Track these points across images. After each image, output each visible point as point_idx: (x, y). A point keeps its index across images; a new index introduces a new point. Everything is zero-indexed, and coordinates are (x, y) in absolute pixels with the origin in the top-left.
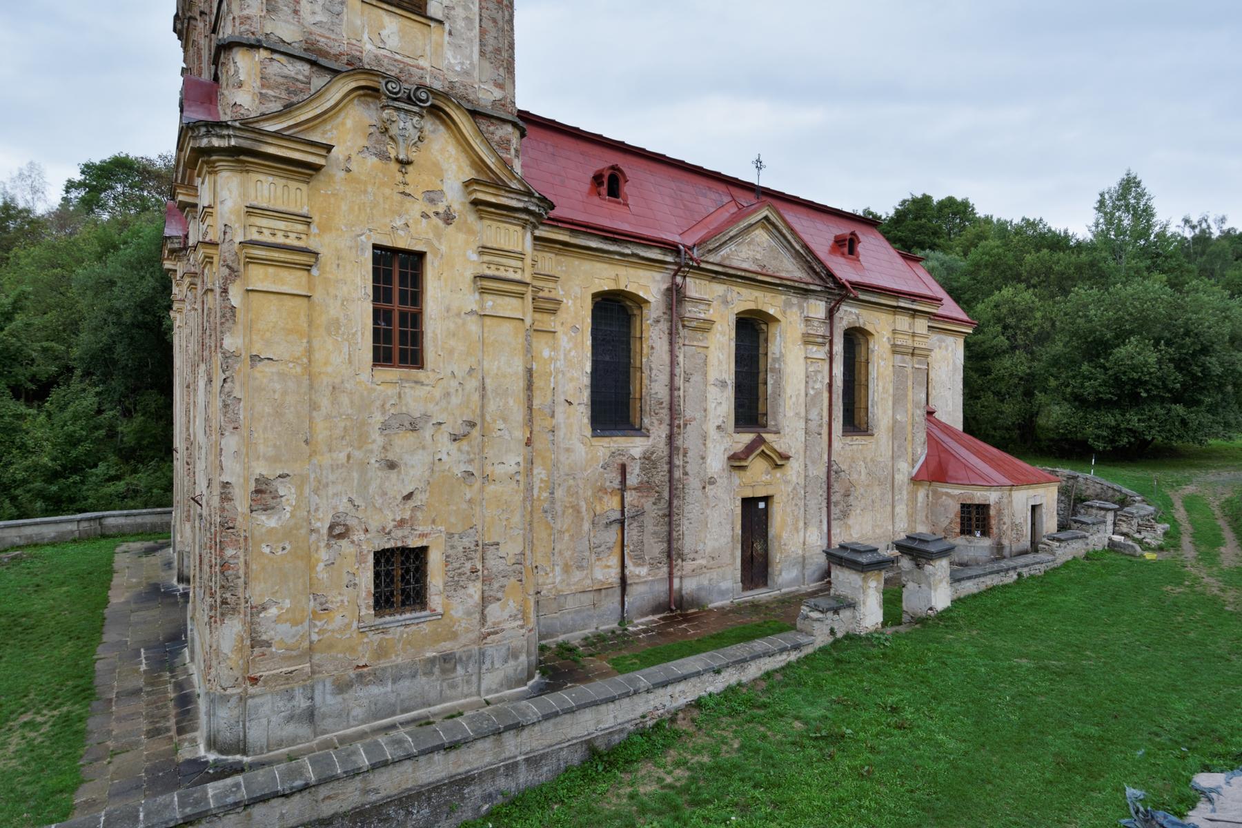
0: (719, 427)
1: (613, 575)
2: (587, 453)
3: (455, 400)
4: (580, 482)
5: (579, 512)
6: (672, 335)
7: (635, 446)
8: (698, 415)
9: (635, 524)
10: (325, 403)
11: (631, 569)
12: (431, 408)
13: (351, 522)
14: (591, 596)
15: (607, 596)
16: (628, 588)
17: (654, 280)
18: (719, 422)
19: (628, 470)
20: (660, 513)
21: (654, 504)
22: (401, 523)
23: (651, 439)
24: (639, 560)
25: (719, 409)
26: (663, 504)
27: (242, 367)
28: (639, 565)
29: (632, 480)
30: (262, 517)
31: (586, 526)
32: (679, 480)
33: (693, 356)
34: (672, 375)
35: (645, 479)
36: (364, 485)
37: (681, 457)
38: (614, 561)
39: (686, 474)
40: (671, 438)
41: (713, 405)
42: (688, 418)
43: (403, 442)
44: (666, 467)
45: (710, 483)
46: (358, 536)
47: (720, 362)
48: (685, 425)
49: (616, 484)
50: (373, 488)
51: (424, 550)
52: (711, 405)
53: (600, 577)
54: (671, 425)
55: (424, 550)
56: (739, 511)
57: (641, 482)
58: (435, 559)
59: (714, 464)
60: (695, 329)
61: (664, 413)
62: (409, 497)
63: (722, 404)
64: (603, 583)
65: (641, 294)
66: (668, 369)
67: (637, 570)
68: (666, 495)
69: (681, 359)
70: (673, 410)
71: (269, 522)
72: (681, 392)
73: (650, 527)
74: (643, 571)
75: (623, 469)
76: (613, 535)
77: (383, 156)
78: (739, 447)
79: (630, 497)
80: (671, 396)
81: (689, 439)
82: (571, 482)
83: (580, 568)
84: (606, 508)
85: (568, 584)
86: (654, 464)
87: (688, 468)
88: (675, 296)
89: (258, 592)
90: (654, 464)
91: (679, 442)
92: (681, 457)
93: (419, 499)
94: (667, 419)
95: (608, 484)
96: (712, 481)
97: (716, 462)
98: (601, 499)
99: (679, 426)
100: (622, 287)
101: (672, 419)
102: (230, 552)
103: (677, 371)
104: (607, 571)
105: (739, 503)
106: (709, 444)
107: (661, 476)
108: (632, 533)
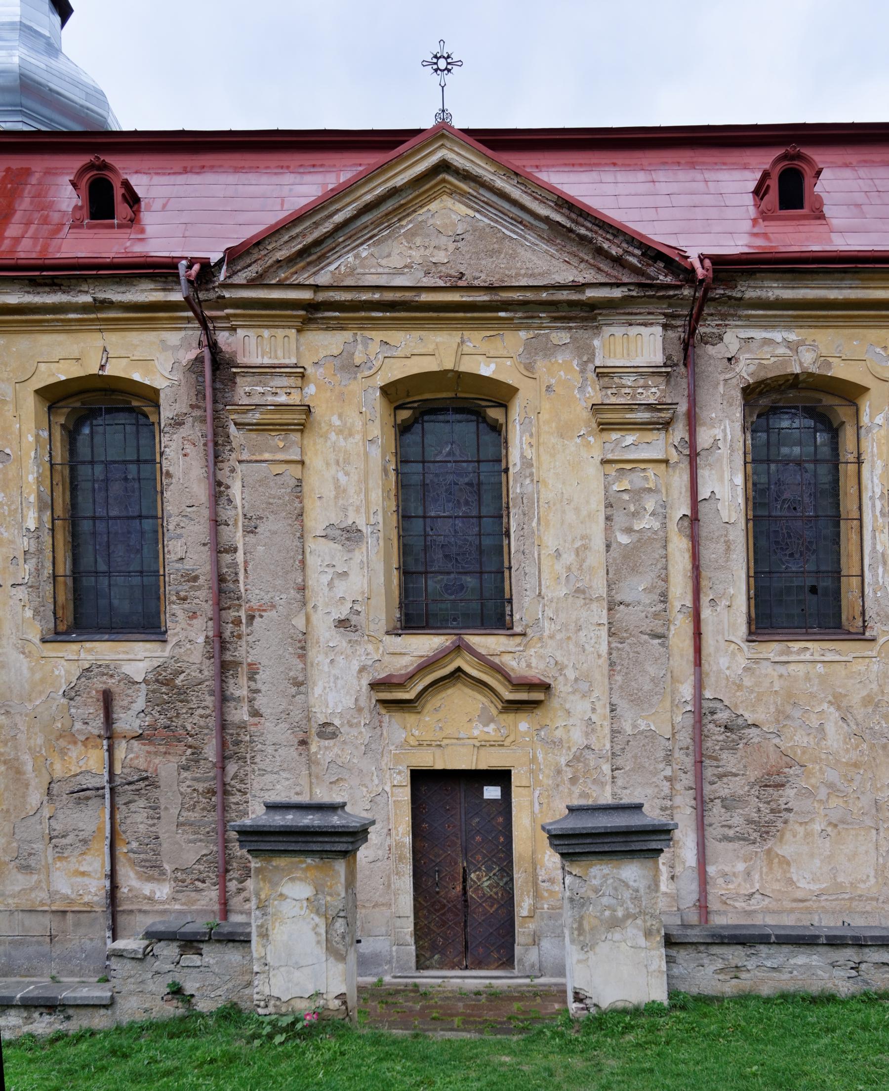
0: (343, 624)
1: (94, 888)
2: (32, 670)
4: (18, 719)
5: (19, 772)
6: (217, 448)
7: (136, 659)
8: (281, 599)
9: (142, 803)
11: (131, 881)
14: (46, 920)
15: (77, 925)
16: (122, 920)
17: (164, 346)
18: (343, 612)
19: (119, 703)
20: (201, 786)
21: (186, 768)
23: (169, 647)
24: (152, 869)
25: (341, 588)
26: (206, 769)
28: (150, 879)
29: (128, 720)
31: (35, 797)
32: (243, 726)
33: (262, 482)
34: (216, 523)
35: (163, 721)
37: (243, 680)
38: (96, 863)
39: (255, 713)
40: (220, 644)
41: (325, 579)
42: (254, 604)
44: (209, 701)
45: (321, 735)
47: (340, 491)
48: (251, 618)
49: (97, 726)
52: (318, 580)
53: (66, 890)
54: (218, 620)
56: (405, 795)
57: (153, 727)
59: (332, 698)
60: (261, 427)
61: (202, 598)
63: (357, 575)
64: (72, 902)
65: (137, 377)
66: (206, 513)
67: (147, 889)
68: (210, 752)
69: (236, 491)
70: (223, 590)
72: (240, 556)
73: (172, 811)
74: (163, 891)
75: (107, 699)
76: (94, 819)
78: (403, 664)
79: (121, 752)
80: (217, 564)
81: (261, 646)
83: (26, 869)
84: (75, 770)
86: (182, 694)
87: (261, 702)
88: (217, 370)
90: (182, 694)
91: (242, 652)
92: (243, 680)
94: (208, 608)
95: (78, 725)
96: (327, 731)
97: (337, 687)
98: (63, 752)
99: (237, 622)
100: (94, 370)
101: (220, 608)
103: (226, 513)
104: (80, 879)
105: (405, 779)
106: (318, 657)
107: (198, 715)
108: (137, 819)
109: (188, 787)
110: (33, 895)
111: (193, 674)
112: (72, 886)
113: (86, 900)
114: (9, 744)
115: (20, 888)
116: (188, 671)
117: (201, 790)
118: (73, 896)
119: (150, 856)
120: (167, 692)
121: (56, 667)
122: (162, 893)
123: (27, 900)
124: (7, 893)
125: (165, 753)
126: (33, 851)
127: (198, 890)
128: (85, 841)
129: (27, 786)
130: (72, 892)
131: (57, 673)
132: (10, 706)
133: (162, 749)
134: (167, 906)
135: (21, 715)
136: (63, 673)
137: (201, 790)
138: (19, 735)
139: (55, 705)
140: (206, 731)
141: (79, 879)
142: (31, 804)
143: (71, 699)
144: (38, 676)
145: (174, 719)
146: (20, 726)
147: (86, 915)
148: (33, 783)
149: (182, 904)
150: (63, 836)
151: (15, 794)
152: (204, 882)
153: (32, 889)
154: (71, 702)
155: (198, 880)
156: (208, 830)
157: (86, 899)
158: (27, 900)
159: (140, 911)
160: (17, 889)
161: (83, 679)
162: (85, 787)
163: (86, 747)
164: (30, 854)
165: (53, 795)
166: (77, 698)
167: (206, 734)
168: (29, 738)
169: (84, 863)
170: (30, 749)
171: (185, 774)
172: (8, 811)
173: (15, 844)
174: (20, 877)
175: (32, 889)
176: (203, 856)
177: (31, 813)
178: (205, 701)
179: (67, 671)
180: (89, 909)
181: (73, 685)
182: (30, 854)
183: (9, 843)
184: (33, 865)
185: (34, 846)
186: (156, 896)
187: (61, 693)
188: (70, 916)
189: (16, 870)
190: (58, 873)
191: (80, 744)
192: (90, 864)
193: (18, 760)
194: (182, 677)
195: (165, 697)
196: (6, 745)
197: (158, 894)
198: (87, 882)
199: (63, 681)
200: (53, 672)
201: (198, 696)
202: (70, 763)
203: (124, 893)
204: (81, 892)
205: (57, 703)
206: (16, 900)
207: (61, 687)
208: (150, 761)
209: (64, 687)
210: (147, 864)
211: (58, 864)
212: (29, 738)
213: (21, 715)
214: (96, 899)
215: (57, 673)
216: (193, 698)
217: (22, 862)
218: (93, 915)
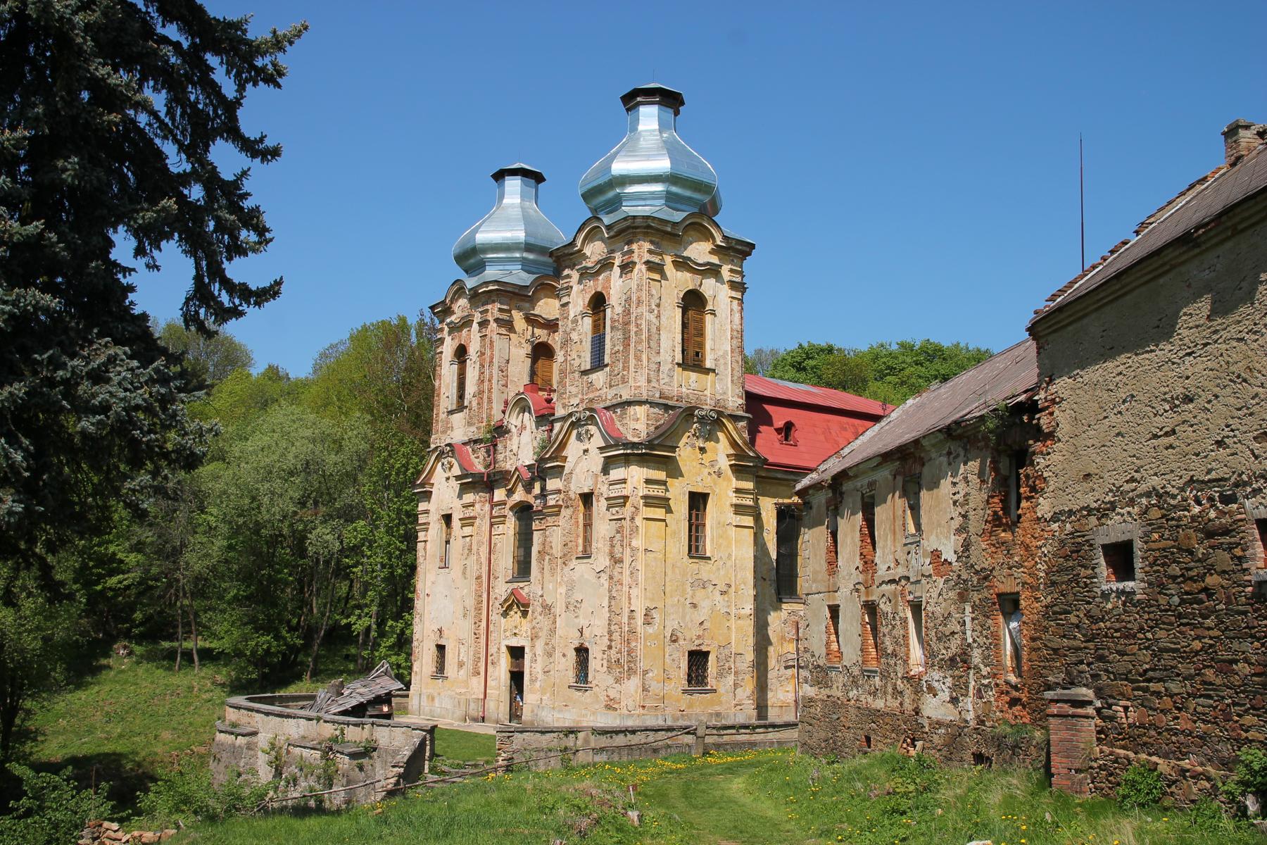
3: (722, 572)
10: (669, 572)
12: (712, 577)
13: (679, 634)
22: (699, 637)
27: (640, 555)
30: (647, 627)
36: (684, 617)
43: (700, 593)
46: (681, 642)
50: (688, 618)
51: (708, 653)
55: (708, 653)
58: (711, 658)
62: (701, 623)
71: (650, 630)
77: (693, 446)
89: (642, 665)
93: (706, 625)
102: (633, 644)
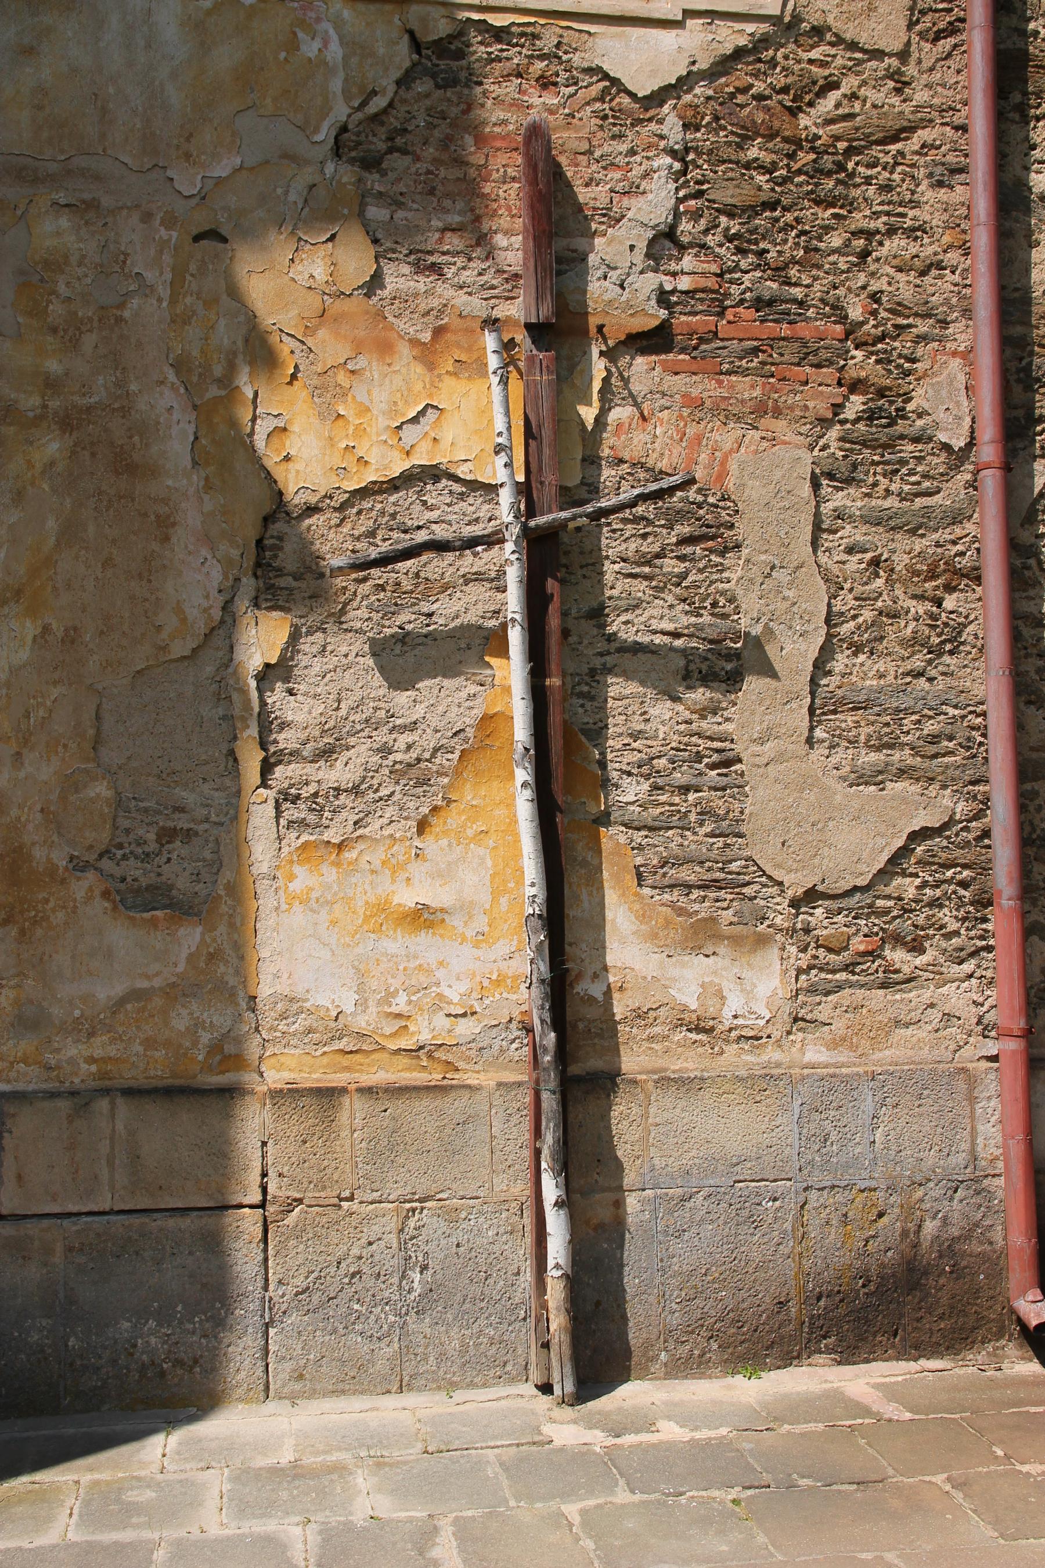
5: (130, 466)
24: (718, 897)
28: (701, 937)
64: (362, 1046)
67: (691, 981)
74: (755, 986)
82: (54, 231)
85: (29, 1021)
86: (831, 170)
90: (831, 170)
109: (850, 550)
110: (180, 1022)
111: (873, 96)
112: (361, 975)
113: (425, 1037)
114: (89, 340)
115: (119, 989)
116: (849, 84)
117: (901, 562)
118: (361, 1022)
119: (697, 841)
120: (767, 158)
121: (302, 23)
122: (749, 994)
123: (149, 1043)
124: (56, 1011)
125: (760, 410)
126: (182, 822)
127: (891, 981)
128: (415, 774)
129: (165, 527)
130: (361, 1004)
131: (311, 49)
132: (97, 178)
133: (748, 389)
134: (771, 1054)
135: (147, 217)
136: (335, 51)
137: (901, 562)
138: (135, 302)
139: (299, 185)
140: (923, 327)
141: (395, 943)
142: (179, 610)
143: (371, 163)
144: (225, 57)
145: (793, 272)
146: (138, 264)
147: (424, 1104)
148: (191, 517)
149: (834, 1045)
150: (326, 754)
151: (108, 563)
152: (916, 947)
153: (176, 993)
154: (374, 182)
155: (897, 940)
156: (930, 727)
157: (423, 1032)
158: (149, 1043)
159: (664, 1081)
160: (106, 992)
161: (422, 86)
162: (422, 536)
163: (431, 366)
164: (167, 835)
165: (280, 572)
166: (398, 162)
167: (922, 339)
168: (180, 320)
169: (416, 869)
170: (180, 366)
171: (838, 499)
172: (71, 637)
173: (101, 789)
174: (121, 936)
175: (176, 993)
176: (917, 836)
177: (179, 649)
178: (915, 204)
179: (355, 48)
180: (435, 1077)
181: (379, 103)
182: (167, 835)
183: (71, 783)
184: (182, 883)
185: (189, 797)
186: (727, 1013)
187: (325, 133)
188: (353, 1111)
189: (101, 905)
190: (298, 918)
191: (405, 350)
192: (443, 875)
193: (125, 411)
194: (827, 104)
195: (761, 179)
196: (75, 344)
197: (734, 1003)
198: (431, 958)
199: (336, 85)
200: (293, 45)
201: (886, 188)
202: (360, 431)
203: (592, 1000)
204: (400, 1003)
205: (308, 175)
206: (100, 1046)
207: (324, 114)
208: (699, 438)
209: (341, 112)
210: (687, 874)
211: (303, 878)
212: (180, 320)
213: (147, 217)
214: (466, 1028)
215: (311, 49)
216: (871, 190)
217: (133, 869)
218: (456, 1106)
